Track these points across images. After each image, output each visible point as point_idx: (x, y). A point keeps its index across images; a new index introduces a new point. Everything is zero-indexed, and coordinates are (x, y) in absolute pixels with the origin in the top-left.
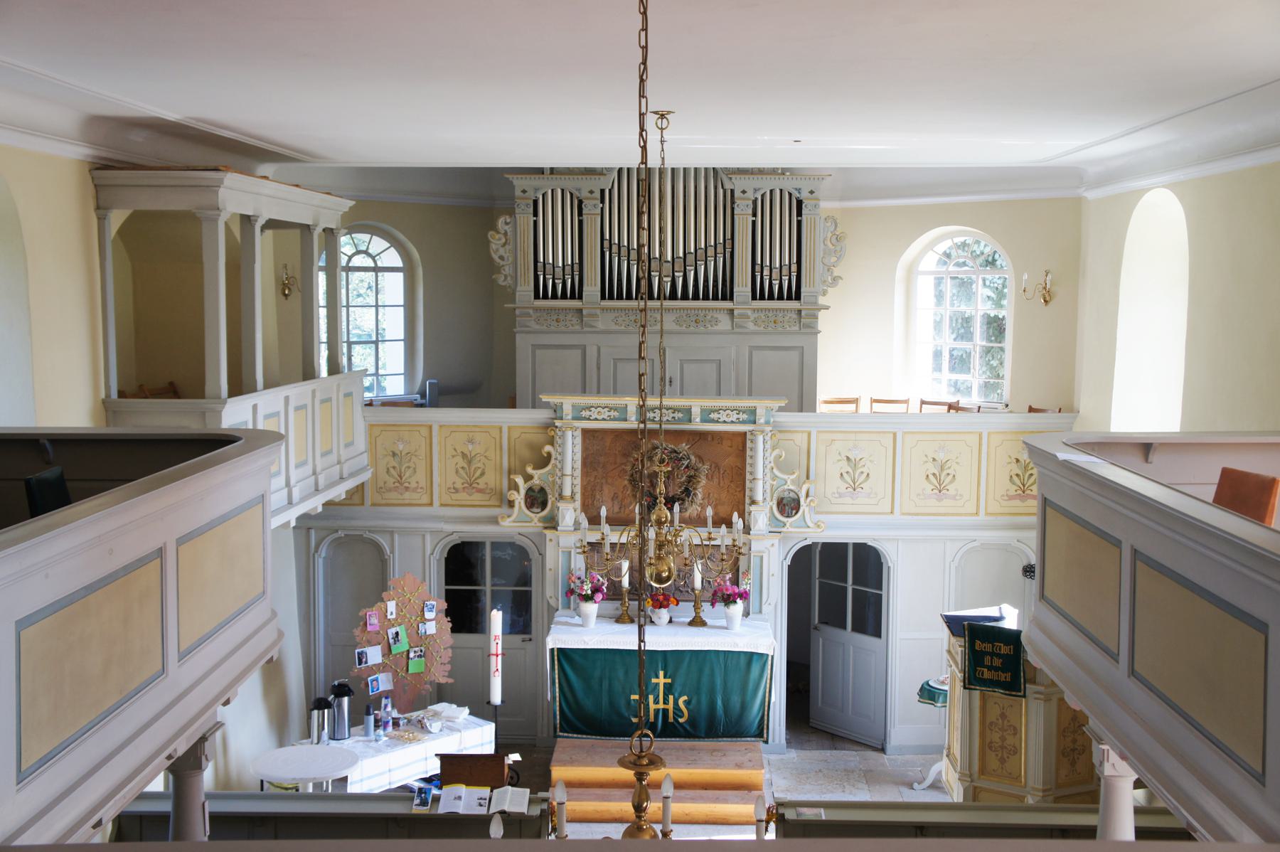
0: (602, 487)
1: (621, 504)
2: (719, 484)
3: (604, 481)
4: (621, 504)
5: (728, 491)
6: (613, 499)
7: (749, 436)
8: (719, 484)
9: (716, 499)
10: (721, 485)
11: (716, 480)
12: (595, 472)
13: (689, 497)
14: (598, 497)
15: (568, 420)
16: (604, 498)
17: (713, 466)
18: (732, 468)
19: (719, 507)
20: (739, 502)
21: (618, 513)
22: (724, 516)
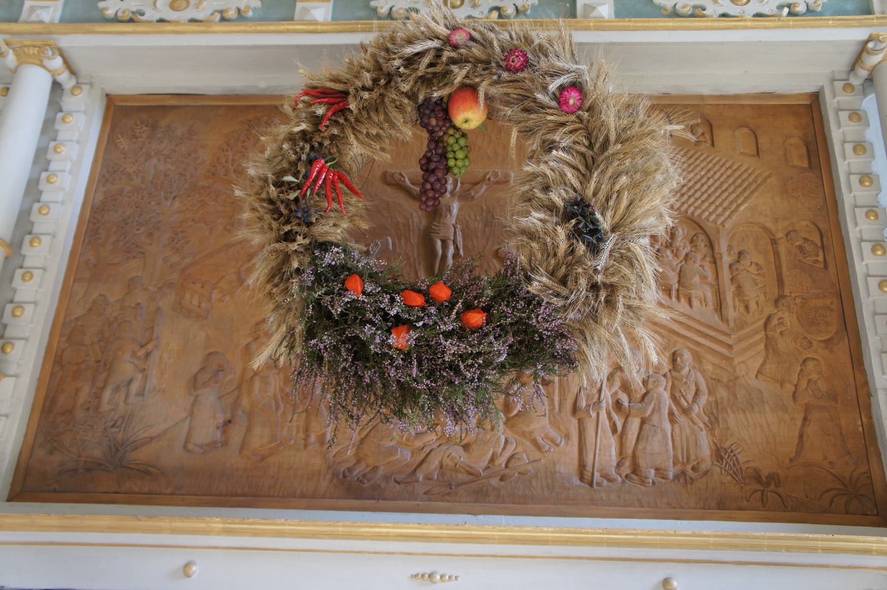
0: (152, 329)
1: (236, 405)
2: (720, 307)
3: (166, 303)
4: (236, 405)
5: (769, 343)
6: (194, 383)
7: (830, 103)
8: (720, 307)
9: (714, 382)
10: (731, 313)
11: (703, 291)
12: (134, 263)
13: (595, 250)
14: (126, 368)
15: (41, 22)
16: (153, 381)
17: (680, 233)
18: (774, 242)
19: (732, 420)
20: (833, 397)
21: (213, 445)
22: (767, 467)
